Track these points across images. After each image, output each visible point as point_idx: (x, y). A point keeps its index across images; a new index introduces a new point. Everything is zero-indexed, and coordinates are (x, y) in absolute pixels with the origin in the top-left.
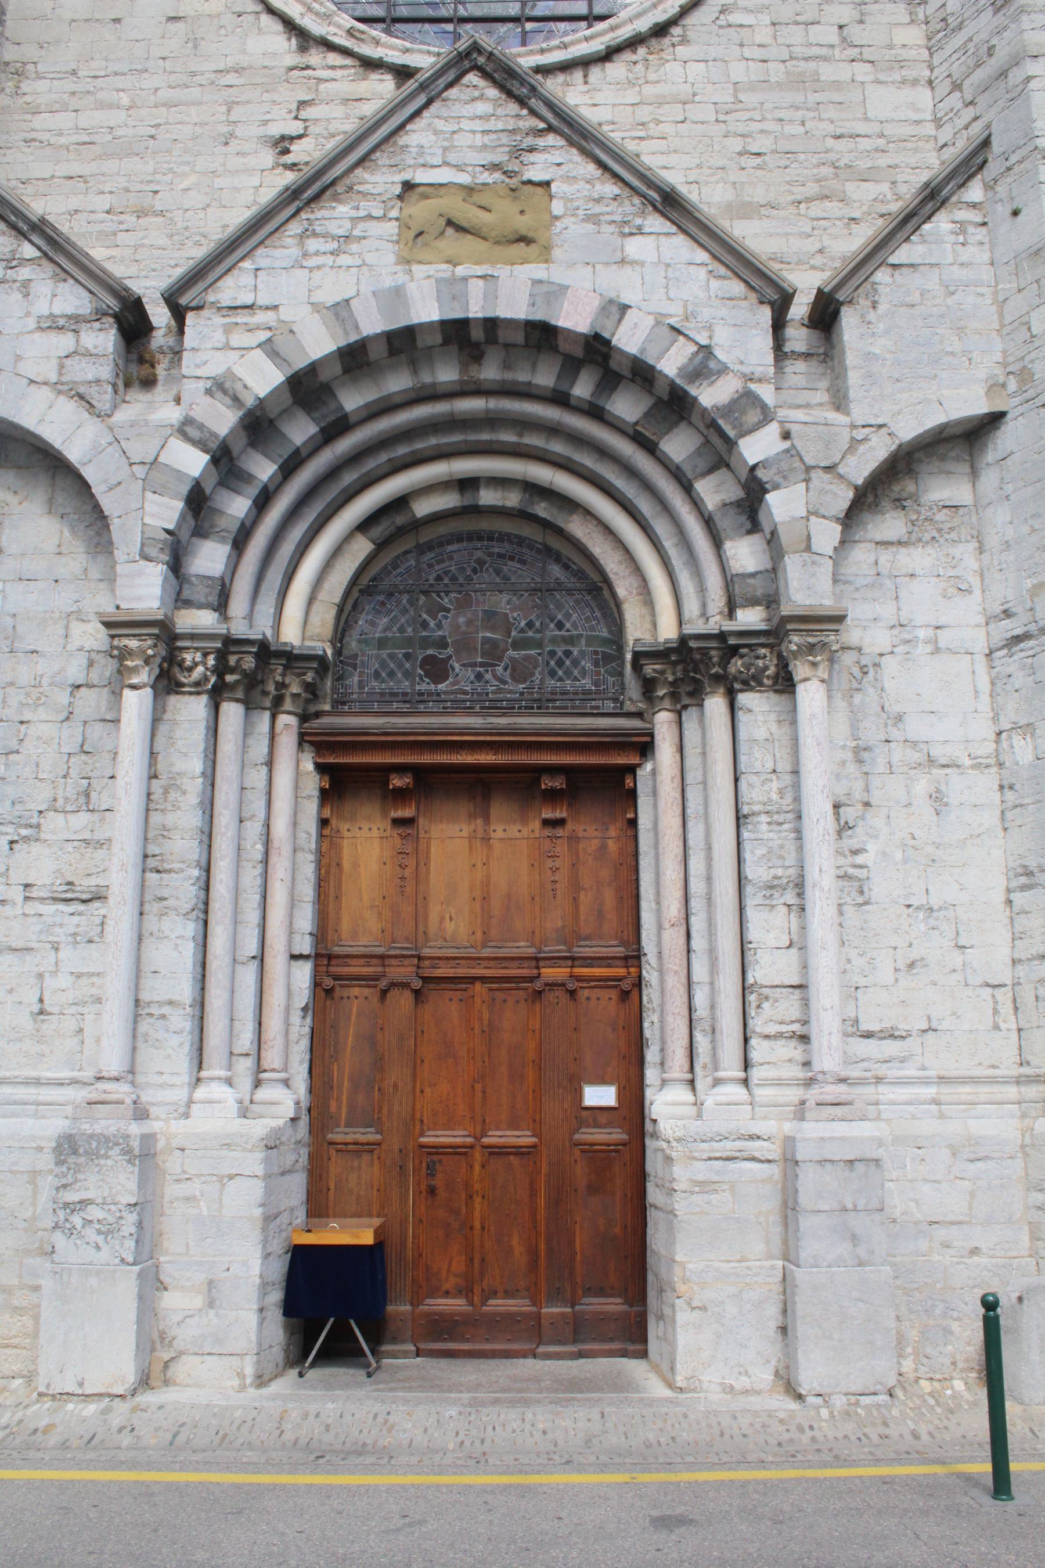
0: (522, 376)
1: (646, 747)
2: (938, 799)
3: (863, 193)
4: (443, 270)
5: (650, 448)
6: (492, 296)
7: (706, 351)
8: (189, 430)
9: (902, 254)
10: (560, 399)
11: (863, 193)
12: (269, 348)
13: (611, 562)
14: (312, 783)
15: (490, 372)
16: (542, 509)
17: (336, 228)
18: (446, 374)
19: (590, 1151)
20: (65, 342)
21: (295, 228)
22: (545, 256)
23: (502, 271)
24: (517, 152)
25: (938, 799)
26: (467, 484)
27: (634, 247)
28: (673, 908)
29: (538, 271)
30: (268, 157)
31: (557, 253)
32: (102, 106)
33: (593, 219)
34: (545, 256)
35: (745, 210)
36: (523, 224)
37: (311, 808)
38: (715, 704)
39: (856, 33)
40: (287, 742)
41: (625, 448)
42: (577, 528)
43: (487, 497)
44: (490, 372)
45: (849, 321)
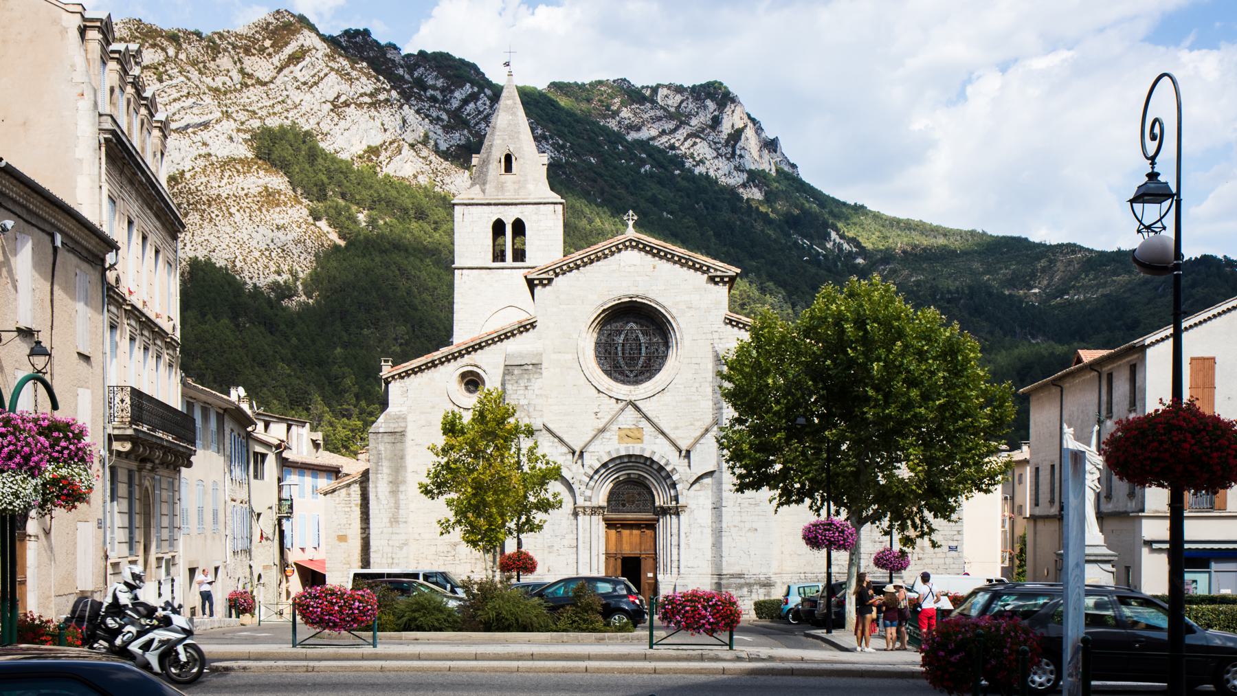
0: (638, 460)
1: (658, 521)
2: (702, 532)
3: (698, 424)
4: (626, 445)
5: (659, 473)
6: (633, 450)
7: (668, 461)
8: (585, 474)
9: (701, 441)
10: (645, 464)
11: (698, 424)
12: (598, 459)
13: (655, 493)
14: (605, 526)
15: (633, 460)
16: (641, 478)
17: (608, 437)
18: (626, 460)
19: (648, 583)
20: (564, 458)
21: (601, 437)
22: (642, 442)
23: (635, 445)
24: (637, 422)
25: (702, 532)
26: (628, 474)
27: (657, 441)
28: (661, 547)
29: (641, 445)
30: (594, 416)
31: (645, 442)
32: (564, 405)
33: (650, 435)
34: (642, 442)
35: (677, 428)
36: (639, 436)
37: (605, 530)
38: (668, 516)
39: (700, 389)
40: (601, 520)
41: (655, 472)
42: (647, 482)
43: (632, 476)
44: (633, 460)
45: (692, 453)
